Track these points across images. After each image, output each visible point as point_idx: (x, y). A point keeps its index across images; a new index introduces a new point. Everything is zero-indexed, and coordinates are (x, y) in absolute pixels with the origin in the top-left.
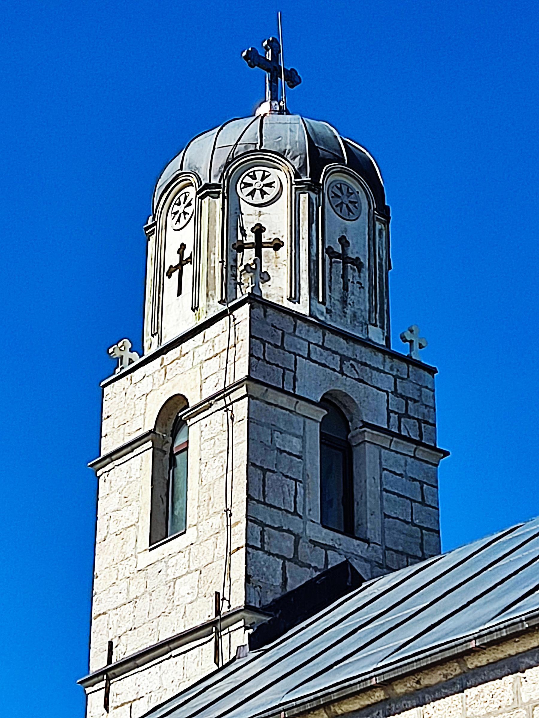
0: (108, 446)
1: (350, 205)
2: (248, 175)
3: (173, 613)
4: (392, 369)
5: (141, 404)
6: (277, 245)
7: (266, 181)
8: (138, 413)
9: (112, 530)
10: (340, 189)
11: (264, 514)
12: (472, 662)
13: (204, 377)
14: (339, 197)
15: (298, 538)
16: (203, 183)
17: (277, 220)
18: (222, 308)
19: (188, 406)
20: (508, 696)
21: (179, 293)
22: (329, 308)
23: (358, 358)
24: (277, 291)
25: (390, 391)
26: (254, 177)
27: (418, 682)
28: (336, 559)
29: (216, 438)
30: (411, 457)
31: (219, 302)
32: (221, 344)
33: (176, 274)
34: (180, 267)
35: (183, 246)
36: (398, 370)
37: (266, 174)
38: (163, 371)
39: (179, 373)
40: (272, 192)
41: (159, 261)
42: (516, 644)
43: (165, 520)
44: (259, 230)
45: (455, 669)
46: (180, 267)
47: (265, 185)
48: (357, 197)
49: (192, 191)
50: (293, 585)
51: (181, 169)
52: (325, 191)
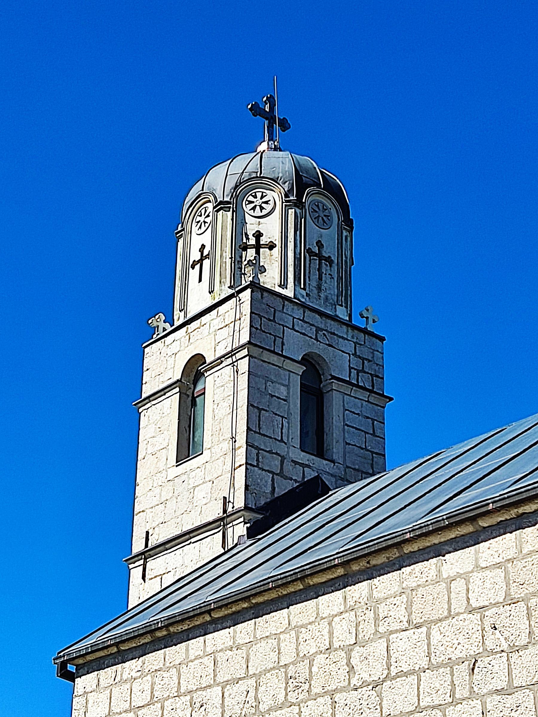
0: (147, 391)
1: (324, 218)
2: (251, 195)
3: (193, 512)
4: (353, 337)
5: (171, 360)
6: (271, 246)
7: (264, 200)
8: (169, 367)
9: (149, 452)
10: (318, 206)
11: (259, 441)
12: (408, 549)
13: (217, 342)
14: (316, 212)
15: (283, 458)
16: (218, 201)
17: (271, 228)
18: (231, 291)
19: (205, 363)
20: (433, 573)
21: (200, 280)
22: (308, 292)
23: (328, 329)
24: (270, 279)
25: (351, 353)
26: (255, 197)
27: (368, 563)
28: (310, 474)
29: (225, 386)
30: (366, 401)
31: (229, 287)
32: (230, 317)
33: (198, 267)
35: (203, 246)
36: (357, 338)
37: (264, 194)
38: (187, 337)
39: (199, 338)
40: (268, 208)
41: (186, 257)
42: (439, 536)
43: (188, 445)
44: (258, 235)
45: (395, 553)
47: (263, 203)
48: (329, 212)
49: (210, 206)
50: (279, 492)
51: (203, 190)
52: (307, 207)
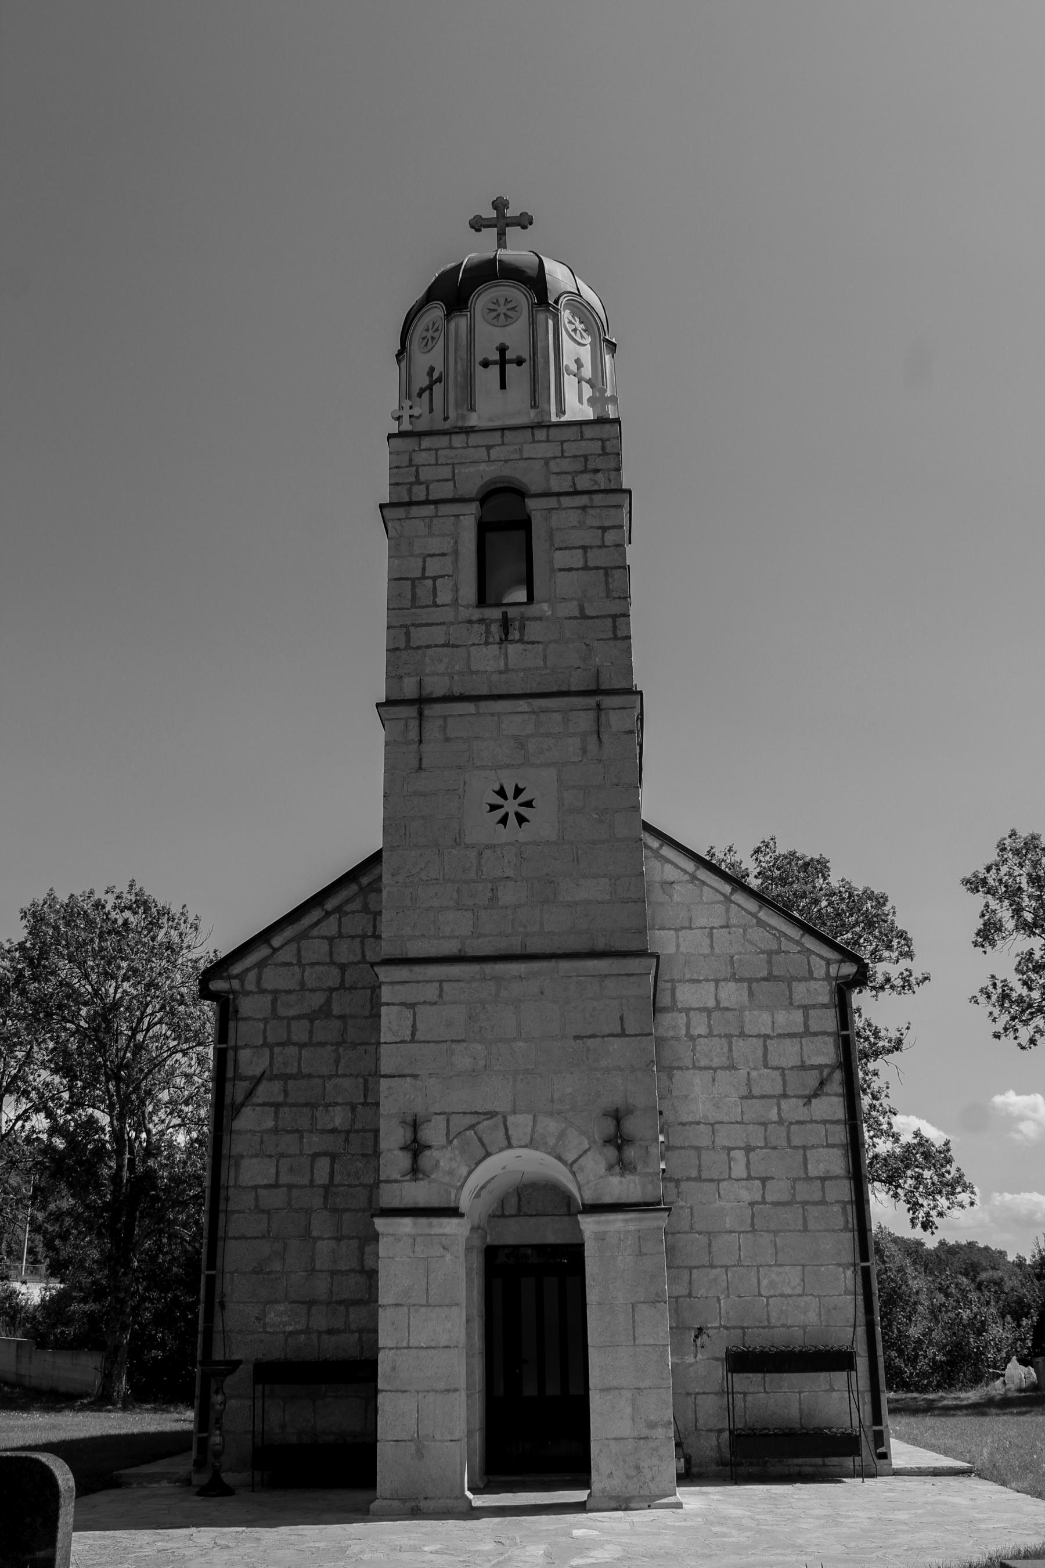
34: (430, 388)
35: (432, 369)
44: (502, 350)
46: (430, 388)
